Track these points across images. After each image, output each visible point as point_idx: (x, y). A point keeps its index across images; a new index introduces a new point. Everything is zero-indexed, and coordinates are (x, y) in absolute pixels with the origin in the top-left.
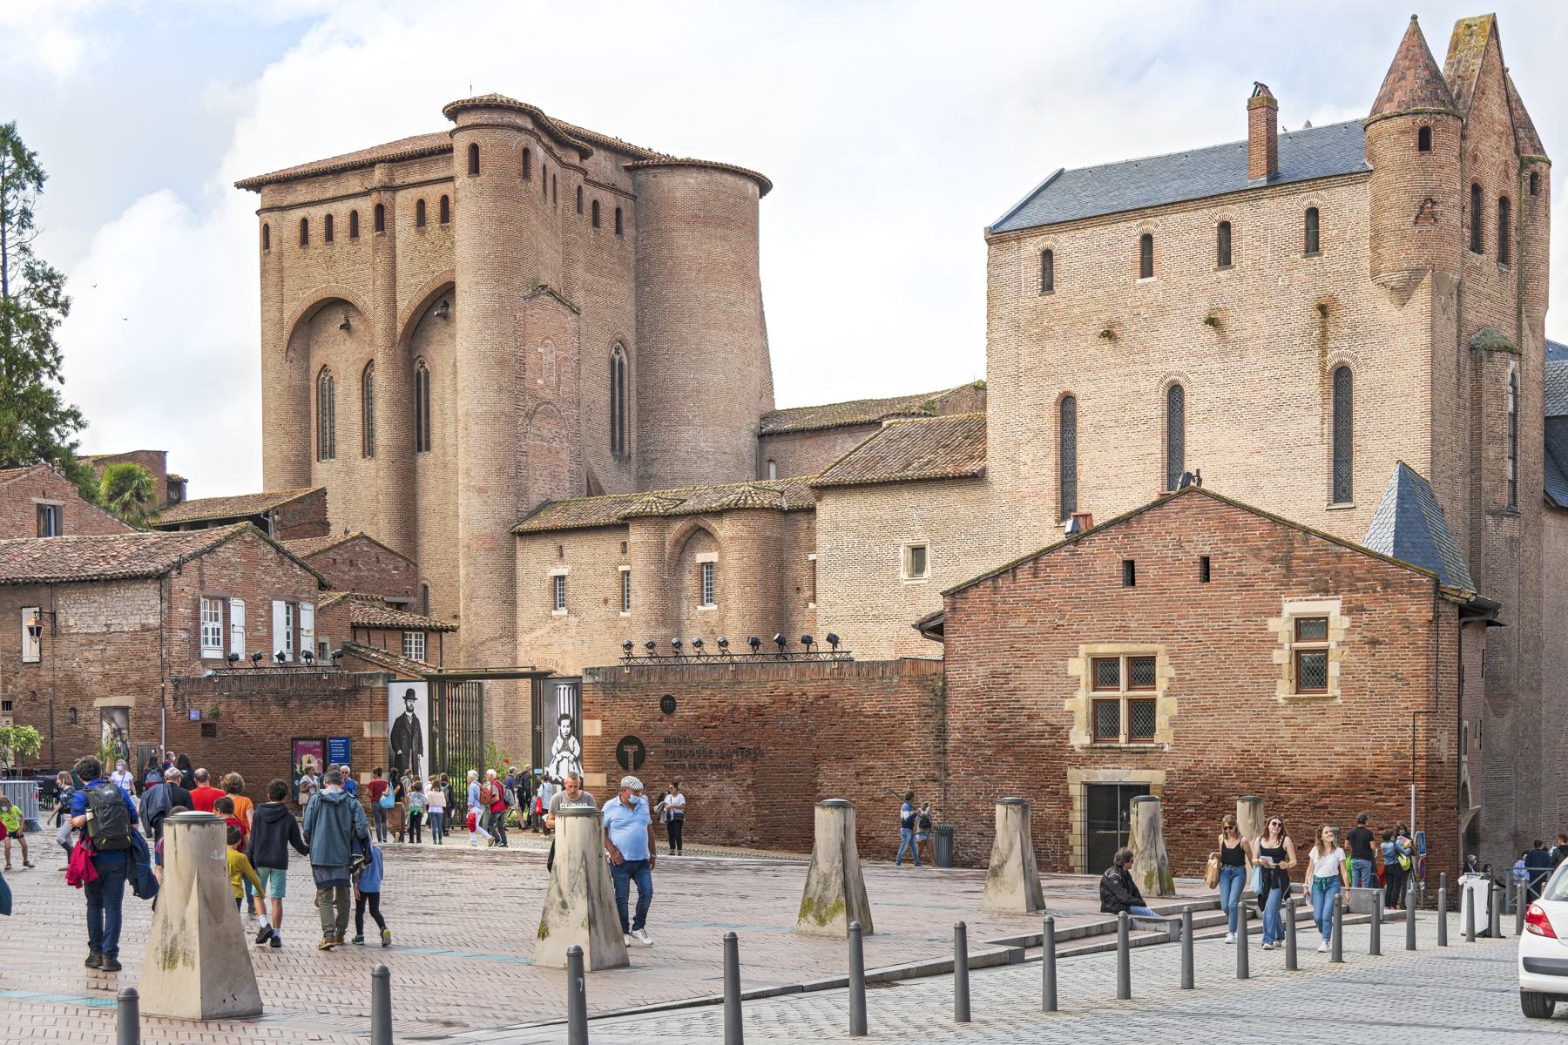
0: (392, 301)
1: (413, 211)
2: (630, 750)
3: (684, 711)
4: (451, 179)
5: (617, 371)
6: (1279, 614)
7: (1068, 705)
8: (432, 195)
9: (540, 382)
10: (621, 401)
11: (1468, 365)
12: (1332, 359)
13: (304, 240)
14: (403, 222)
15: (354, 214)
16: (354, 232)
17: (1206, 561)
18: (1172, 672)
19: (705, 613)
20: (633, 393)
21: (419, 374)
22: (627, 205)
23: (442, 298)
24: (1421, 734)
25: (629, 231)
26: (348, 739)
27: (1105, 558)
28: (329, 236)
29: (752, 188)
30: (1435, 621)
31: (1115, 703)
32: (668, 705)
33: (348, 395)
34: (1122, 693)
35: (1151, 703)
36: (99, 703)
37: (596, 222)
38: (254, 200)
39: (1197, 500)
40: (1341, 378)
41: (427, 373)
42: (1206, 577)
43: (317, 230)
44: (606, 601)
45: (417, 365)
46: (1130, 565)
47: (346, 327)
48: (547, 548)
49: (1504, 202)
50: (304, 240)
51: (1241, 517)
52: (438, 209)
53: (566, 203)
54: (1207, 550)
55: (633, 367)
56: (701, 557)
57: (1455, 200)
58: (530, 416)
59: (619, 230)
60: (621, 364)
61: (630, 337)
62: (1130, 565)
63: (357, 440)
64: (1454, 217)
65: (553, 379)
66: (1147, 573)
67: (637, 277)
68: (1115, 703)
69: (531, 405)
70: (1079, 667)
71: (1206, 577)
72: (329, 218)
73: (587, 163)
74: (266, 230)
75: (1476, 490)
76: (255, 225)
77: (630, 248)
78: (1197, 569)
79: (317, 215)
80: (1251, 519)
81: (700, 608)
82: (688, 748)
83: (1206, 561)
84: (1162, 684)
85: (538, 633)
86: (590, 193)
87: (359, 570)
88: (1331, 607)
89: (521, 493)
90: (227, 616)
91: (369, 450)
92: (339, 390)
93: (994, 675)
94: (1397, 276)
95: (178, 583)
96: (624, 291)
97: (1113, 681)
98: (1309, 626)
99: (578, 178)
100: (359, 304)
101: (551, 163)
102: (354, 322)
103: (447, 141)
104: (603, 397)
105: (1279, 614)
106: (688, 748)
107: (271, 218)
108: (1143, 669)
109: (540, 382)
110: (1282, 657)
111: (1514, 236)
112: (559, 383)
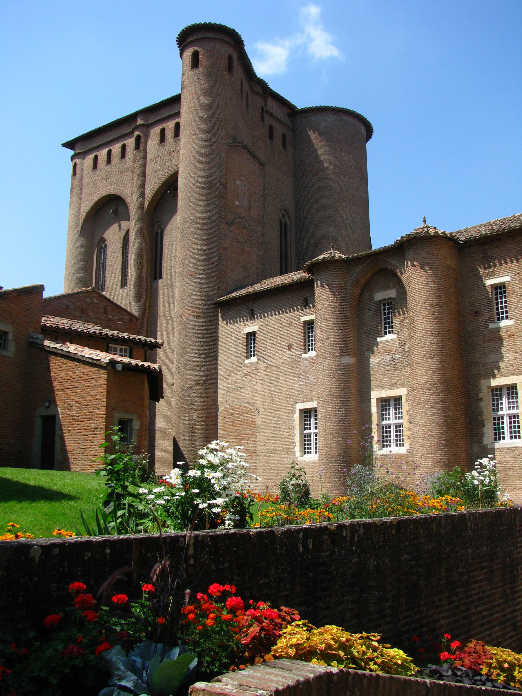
8: (170, 126)
9: (237, 203)
10: (286, 247)
13: (95, 166)
15: (124, 147)
21: (157, 233)
28: (109, 161)
33: (114, 252)
37: (271, 137)
44: (290, 347)
45: (156, 227)
52: (173, 131)
56: (379, 296)
58: (230, 224)
60: (286, 224)
65: (246, 203)
72: (110, 152)
74: (75, 165)
85: (234, 378)
91: (124, 283)
92: (109, 250)
100: (123, 195)
102: (121, 210)
104: (276, 243)
112: (250, 207)
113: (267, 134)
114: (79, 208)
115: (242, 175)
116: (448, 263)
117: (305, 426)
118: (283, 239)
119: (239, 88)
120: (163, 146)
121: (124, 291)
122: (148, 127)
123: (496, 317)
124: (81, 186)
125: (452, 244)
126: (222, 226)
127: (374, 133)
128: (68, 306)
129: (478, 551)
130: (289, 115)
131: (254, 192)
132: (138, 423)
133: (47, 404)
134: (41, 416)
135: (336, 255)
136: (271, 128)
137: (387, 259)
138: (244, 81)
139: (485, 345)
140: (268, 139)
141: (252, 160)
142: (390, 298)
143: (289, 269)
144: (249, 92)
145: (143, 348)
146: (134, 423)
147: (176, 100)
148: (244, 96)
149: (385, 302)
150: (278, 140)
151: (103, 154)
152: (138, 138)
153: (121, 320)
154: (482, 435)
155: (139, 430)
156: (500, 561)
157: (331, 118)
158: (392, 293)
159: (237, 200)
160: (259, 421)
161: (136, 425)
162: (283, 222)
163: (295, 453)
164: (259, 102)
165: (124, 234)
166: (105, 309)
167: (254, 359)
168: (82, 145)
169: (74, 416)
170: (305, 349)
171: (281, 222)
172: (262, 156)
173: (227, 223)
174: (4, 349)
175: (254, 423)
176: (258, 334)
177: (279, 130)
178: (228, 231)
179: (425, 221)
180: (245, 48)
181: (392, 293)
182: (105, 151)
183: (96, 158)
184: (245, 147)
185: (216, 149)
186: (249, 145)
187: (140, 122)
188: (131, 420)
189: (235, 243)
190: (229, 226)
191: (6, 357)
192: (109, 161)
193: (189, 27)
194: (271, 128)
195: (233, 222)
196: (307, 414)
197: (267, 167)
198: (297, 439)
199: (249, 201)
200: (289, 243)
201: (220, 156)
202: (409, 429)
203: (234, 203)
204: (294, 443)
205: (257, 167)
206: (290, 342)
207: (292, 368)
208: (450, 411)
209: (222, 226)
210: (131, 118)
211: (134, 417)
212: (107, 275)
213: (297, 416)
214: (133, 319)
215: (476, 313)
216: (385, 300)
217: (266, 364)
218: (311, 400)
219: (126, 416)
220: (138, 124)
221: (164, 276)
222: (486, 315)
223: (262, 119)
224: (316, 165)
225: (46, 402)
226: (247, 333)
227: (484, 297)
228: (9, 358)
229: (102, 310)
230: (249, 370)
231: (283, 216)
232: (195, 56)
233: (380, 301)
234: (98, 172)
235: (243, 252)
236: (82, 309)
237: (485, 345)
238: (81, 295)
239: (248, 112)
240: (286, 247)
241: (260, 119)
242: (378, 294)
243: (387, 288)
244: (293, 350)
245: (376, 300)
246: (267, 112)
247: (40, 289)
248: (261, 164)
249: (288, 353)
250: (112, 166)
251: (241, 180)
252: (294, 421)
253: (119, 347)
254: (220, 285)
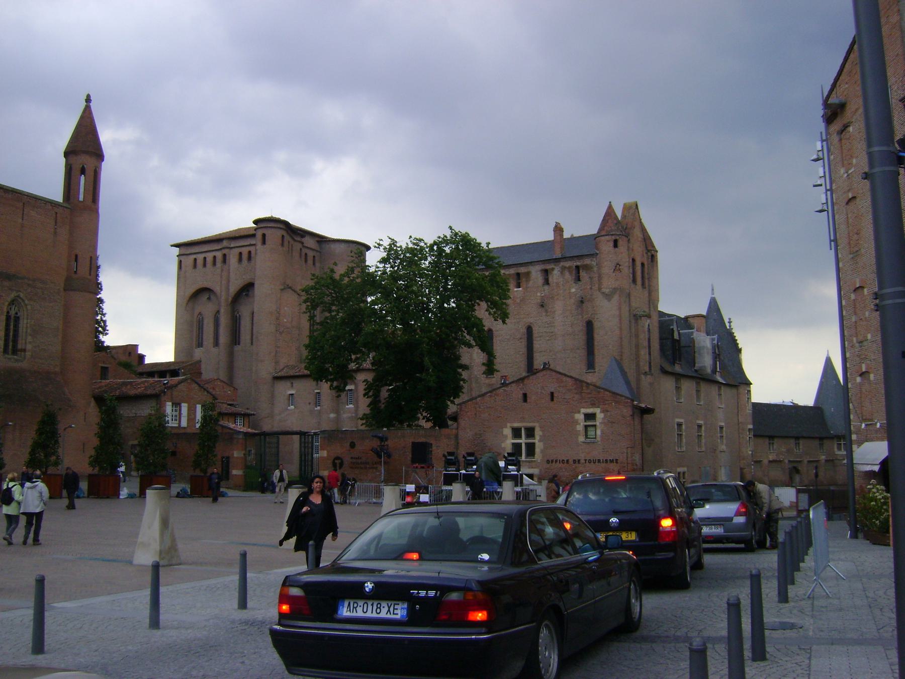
0: (228, 289)
1: (237, 257)
2: (338, 462)
3: (358, 447)
4: (254, 245)
6: (579, 412)
7: (503, 445)
11: (633, 321)
12: (586, 317)
13: (195, 266)
14: (233, 260)
15: (215, 257)
16: (214, 263)
17: (552, 394)
18: (541, 433)
23: (248, 288)
24: (629, 455)
25: (318, 264)
26: (228, 458)
27: (516, 392)
28: (205, 265)
29: (363, 249)
30: (632, 416)
31: (520, 445)
32: (353, 445)
34: (523, 441)
35: (534, 444)
36: (131, 443)
37: (306, 261)
38: (176, 251)
39: (548, 372)
40: (589, 326)
42: (552, 399)
43: (200, 262)
46: (525, 395)
47: (209, 299)
48: (288, 384)
49: (643, 264)
50: (195, 266)
51: (564, 378)
53: (296, 255)
54: (552, 390)
57: (627, 264)
58: (281, 333)
59: (314, 264)
62: (525, 395)
63: (212, 340)
64: (626, 270)
66: (532, 398)
68: (520, 445)
70: (508, 432)
71: (552, 399)
72: (205, 258)
73: (303, 240)
74: (180, 262)
75: (638, 366)
76: (176, 260)
78: (549, 397)
79: (200, 257)
80: (568, 379)
82: (359, 461)
83: (552, 394)
84: (537, 437)
86: (304, 251)
88: (597, 411)
89: (277, 363)
90: (180, 410)
92: (205, 322)
93: (476, 434)
94: (608, 290)
95: (163, 398)
97: (520, 437)
98: (590, 417)
99: (300, 246)
100: (215, 290)
101: (290, 240)
102: (212, 297)
103: (253, 232)
105: (579, 412)
106: (359, 461)
107: (182, 258)
108: (530, 432)
110: (580, 428)
111: (646, 276)
121: (215, 350)
130: (318, 242)
150: (310, 262)
152: (225, 255)
157: (343, 246)
177: (311, 254)
183: (195, 259)
184: (290, 288)
192: (205, 265)
212: (204, 338)
221: (242, 343)
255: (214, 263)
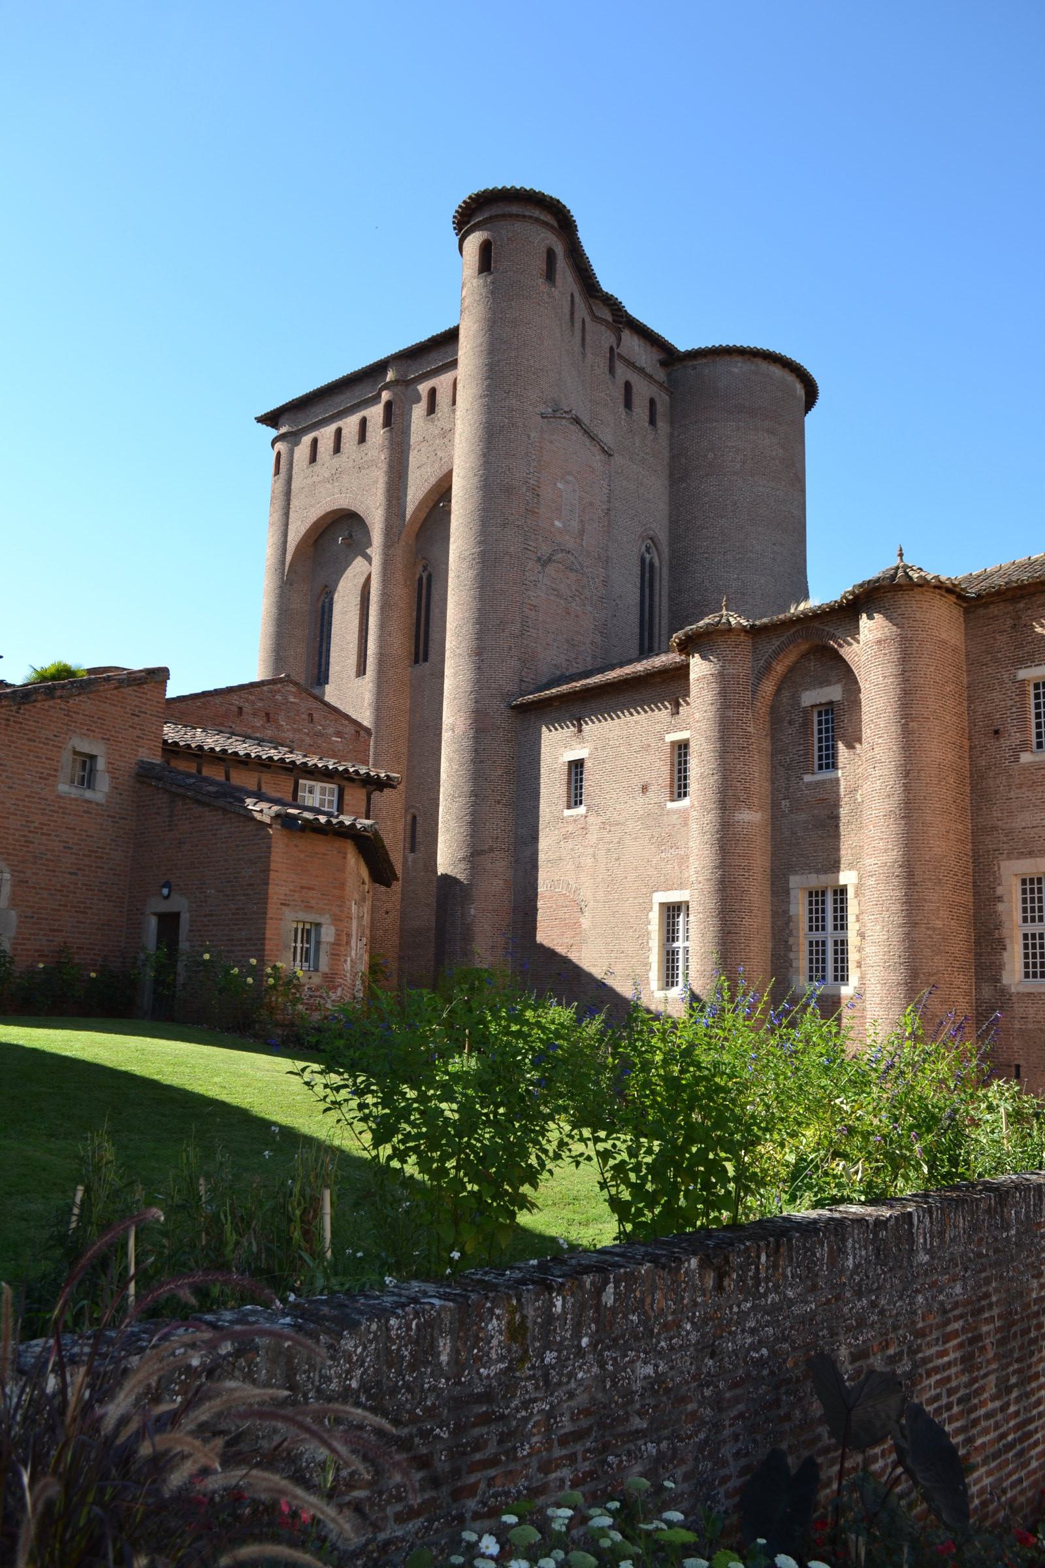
5: (647, 573)
8: (442, 382)
9: (557, 523)
13: (313, 458)
15: (363, 422)
19: (817, 783)
20: (665, 600)
21: (421, 579)
22: (663, 400)
25: (662, 424)
28: (337, 449)
37: (628, 404)
41: (430, 577)
44: (645, 789)
50: (313, 458)
55: (665, 571)
56: (809, 698)
58: (545, 562)
60: (652, 565)
61: (663, 537)
65: (575, 524)
67: (671, 475)
69: (545, 550)
72: (339, 432)
77: (664, 442)
81: (808, 778)
87: (279, 727)
91: (361, 670)
96: (656, 487)
109: (557, 523)
112: (582, 532)
113: (621, 399)
114: (285, 534)
115: (570, 473)
116: (944, 636)
117: (670, 933)
118: (647, 590)
119: (567, 310)
120: (433, 421)
122: (406, 384)
123: (1034, 740)
124: (288, 493)
125: (953, 598)
126: (530, 565)
127: (820, 395)
128: (240, 708)
129: (941, 1298)
130: (664, 364)
131: (591, 504)
132: (333, 929)
133: (165, 891)
134: (155, 914)
135: (731, 619)
136: (628, 386)
137: (827, 629)
138: (578, 299)
139: (1012, 795)
140: (621, 409)
141: (588, 444)
142: (831, 703)
143: (656, 645)
144: (588, 319)
145: (364, 787)
146: (323, 930)
147: (452, 336)
148: (578, 325)
149: (820, 709)
150: (641, 410)
151: (326, 434)
152: (389, 406)
153: (339, 734)
154: (1000, 967)
155: (334, 944)
156: (996, 1311)
158: (834, 693)
159: (559, 519)
160: (585, 922)
161: (328, 934)
162: (648, 561)
163: (648, 984)
164: (607, 338)
165: (362, 580)
166: (311, 715)
167: (582, 810)
168: (291, 418)
169: (212, 915)
170: (672, 793)
171: (643, 560)
172: (607, 436)
173: (539, 559)
174: (89, 787)
175: (577, 924)
176: (588, 765)
177: (643, 390)
178: (541, 576)
179: (901, 555)
180: (580, 234)
181: (834, 693)
182: (330, 430)
183: (315, 442)
184: (577, 421)
185: (520, 424)
186: (585, 419)
187: (390, 376)
188: (318, 925)
189: (552, 598)
190: (544, 565)
191: (90, 802)
192: (337, 449)
193: (477, 195)
194: (628, 386)
195: (550, 560)
196: (672, 911)
197: (618, 459)
198: (655, 958)
199: (582, 521)
200: (657, 599)
201: (529, 437)
202: (860, 950)
203: (553, 525)
204: (647, 965)
205: (598, 458)
206: (646, 779)
207: (648, 828)
208: (938, 918)
209: (530, 565)
210: (380, 368)
211: (325, 919)
213: (655, 916)
214: (362, 733)
215: (996, 732)
216: (821, 704)
217: (600, 819)
218: (681, 886)
219: (311, 917)
220: (388, 380)
222: (1016, 738)
223: (612, 370)
224: (710, 455)
225: (164, 886)
226: (570, 762)
227: (1011, 703)
228: (97, 804)
229: (305, 716)
230: (570, 829)
231: (648, 550)
232: (486, 250)
233: (812, 706)
234: (317, 467)
235: (568, 613)
236: (267, 714)
237: (1012, 795)
238: (265, 688)
239: (584, 355)
240: (651, 606)
241: (607, 370)
242: (808, 693)
243: (824, 682)
244: (650, 794)
245: (803, 705)
246: (620, 356)
247: (159, 676)
248: (608, 453)
249: (641, 799)
250: (342, 458)
251: (567, 482)
252: (649, 923)
253: (318, 786)
254: (523, 674)
255: (362, 439)
